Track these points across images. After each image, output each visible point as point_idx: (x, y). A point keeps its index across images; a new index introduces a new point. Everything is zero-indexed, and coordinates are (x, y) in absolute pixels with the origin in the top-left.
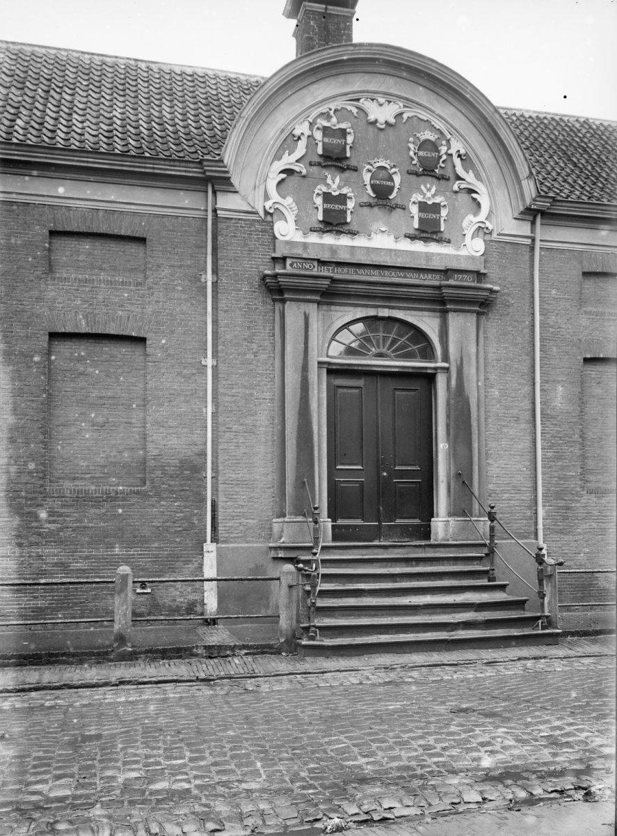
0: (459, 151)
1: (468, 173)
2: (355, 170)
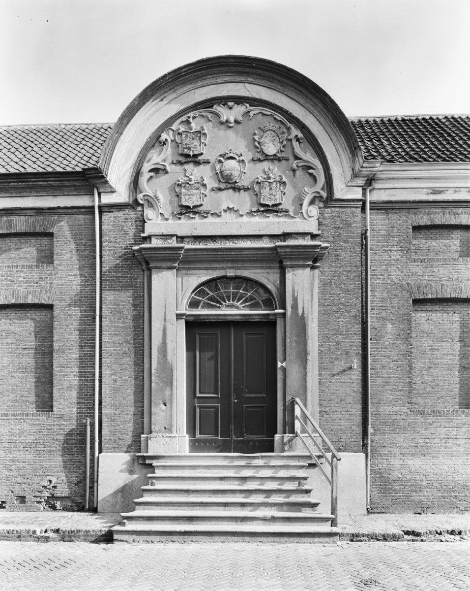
0: (296, 136)
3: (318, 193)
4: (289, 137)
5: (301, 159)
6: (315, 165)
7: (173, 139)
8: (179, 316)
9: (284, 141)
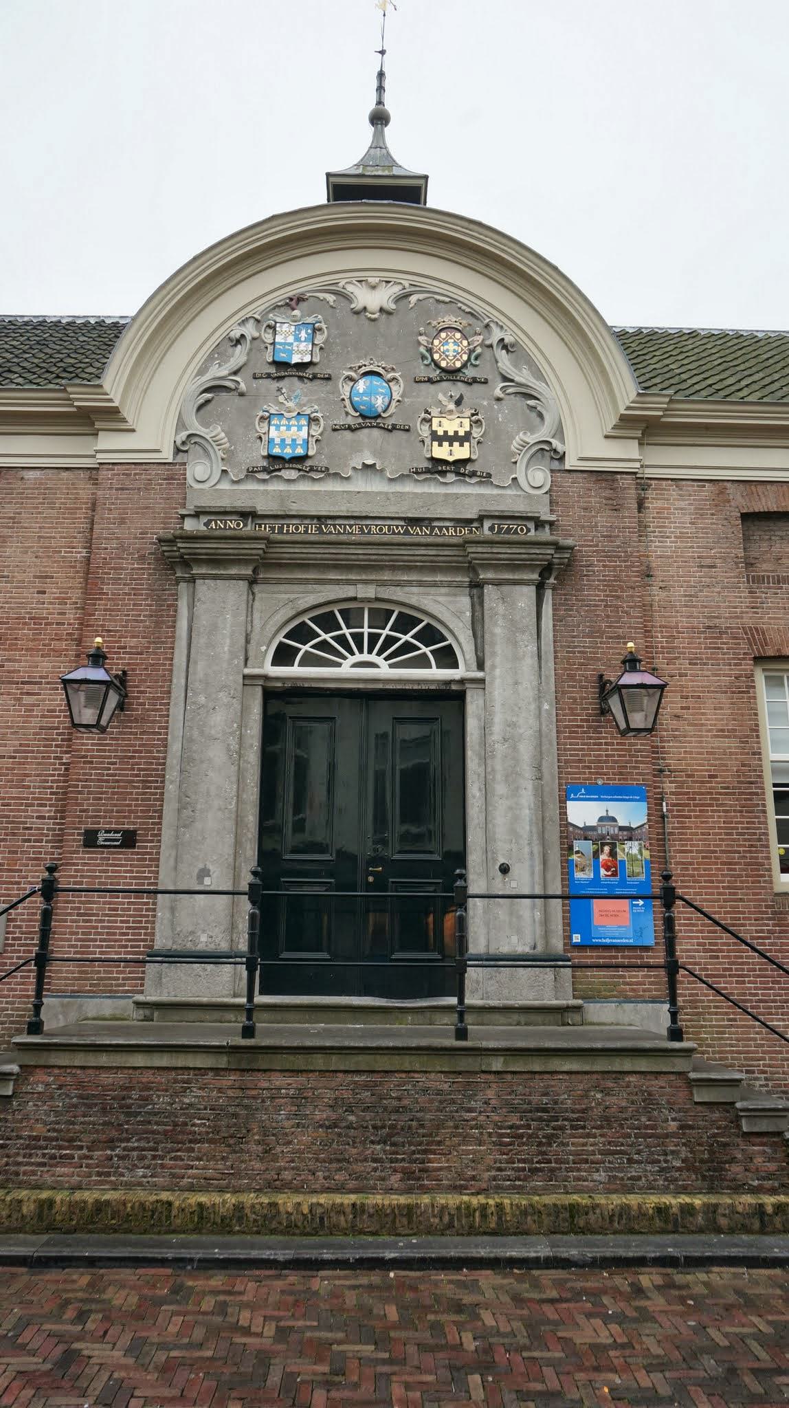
0: (502, 340)
1: (520, 370)
2: (329, 379)
4: (488, 342)
5: (512, 381)
6: (540, 393)
7: (256, 334)
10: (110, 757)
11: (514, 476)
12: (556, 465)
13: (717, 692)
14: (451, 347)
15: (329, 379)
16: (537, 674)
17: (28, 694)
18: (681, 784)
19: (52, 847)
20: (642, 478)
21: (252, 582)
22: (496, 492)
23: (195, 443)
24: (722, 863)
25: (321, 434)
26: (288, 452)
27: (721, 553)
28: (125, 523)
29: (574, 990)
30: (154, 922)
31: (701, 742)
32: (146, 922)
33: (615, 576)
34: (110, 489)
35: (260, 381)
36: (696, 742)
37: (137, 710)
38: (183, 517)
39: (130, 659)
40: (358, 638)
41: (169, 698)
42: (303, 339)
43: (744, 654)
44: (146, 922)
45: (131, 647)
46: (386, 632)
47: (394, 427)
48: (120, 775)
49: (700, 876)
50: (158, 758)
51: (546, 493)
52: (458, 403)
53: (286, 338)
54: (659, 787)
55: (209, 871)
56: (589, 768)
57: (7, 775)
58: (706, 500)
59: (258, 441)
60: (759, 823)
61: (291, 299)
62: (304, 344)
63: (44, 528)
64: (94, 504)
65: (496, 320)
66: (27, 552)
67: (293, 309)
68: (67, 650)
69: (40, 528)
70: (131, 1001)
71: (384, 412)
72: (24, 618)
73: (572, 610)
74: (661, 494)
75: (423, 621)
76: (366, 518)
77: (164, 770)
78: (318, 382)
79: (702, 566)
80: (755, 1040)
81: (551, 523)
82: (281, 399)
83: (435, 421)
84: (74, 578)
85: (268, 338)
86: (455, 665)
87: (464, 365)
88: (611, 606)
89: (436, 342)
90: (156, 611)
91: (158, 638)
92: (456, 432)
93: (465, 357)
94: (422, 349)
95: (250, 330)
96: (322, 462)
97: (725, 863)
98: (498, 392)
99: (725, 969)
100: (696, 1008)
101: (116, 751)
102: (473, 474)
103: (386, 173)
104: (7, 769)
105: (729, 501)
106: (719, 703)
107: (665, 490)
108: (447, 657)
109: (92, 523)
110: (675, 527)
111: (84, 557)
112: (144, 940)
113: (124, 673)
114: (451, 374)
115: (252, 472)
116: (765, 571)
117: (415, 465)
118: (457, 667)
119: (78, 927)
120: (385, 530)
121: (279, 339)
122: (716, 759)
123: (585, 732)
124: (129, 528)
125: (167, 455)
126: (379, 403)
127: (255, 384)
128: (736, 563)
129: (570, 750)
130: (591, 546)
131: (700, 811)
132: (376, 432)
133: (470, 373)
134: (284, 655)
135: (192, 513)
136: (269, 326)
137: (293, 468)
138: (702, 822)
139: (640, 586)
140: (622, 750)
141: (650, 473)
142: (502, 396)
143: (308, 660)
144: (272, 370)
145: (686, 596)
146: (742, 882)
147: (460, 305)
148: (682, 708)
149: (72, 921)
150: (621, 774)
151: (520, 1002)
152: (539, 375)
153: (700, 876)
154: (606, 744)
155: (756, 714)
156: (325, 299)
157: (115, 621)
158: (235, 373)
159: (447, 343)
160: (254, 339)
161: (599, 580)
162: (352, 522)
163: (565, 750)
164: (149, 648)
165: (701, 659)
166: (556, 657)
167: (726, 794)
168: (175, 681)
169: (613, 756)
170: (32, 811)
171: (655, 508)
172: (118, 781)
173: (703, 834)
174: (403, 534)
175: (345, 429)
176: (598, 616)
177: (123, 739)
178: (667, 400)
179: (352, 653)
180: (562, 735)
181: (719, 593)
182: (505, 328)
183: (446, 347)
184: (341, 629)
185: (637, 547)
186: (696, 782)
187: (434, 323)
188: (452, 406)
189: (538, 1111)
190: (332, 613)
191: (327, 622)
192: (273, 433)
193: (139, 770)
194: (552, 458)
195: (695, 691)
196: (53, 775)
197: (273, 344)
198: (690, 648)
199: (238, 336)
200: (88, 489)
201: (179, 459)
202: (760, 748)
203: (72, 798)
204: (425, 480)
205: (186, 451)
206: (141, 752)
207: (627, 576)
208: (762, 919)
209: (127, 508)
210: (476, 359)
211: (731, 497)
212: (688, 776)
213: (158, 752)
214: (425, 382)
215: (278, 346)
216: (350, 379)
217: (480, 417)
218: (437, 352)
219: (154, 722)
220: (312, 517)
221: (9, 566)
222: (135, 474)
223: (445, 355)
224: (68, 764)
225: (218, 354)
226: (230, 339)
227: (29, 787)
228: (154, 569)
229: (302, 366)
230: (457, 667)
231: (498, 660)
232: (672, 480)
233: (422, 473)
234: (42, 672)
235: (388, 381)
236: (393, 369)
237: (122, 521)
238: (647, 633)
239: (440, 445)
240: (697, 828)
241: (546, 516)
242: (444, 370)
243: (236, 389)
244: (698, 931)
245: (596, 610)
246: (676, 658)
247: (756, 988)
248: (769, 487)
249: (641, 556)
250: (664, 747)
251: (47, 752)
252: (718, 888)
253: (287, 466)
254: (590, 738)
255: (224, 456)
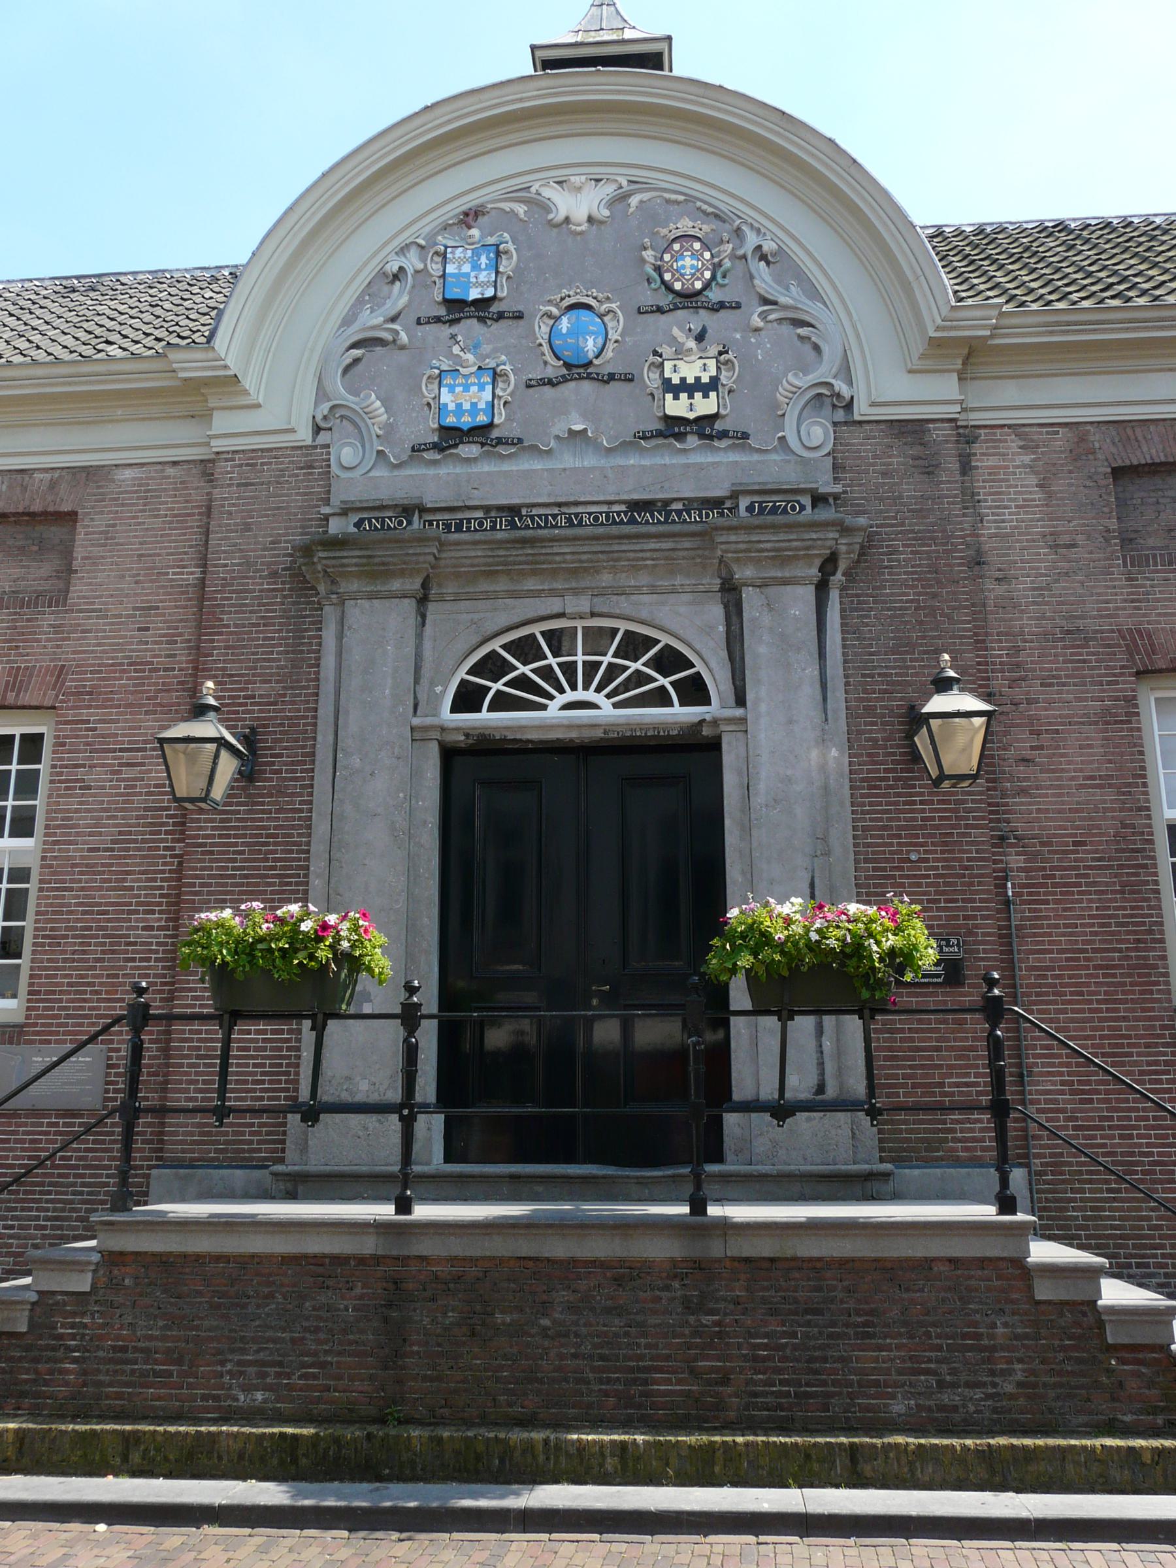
0: (759, 247)
2: (519, 316)
3: (829, 385)
4: (740, 252)
5: (775, 303)
7: (420, 266)
8: (418, 735)
9: (727, 260)
10: (236, 844)
11: (780, 435)
12: (840, 415)
13: (1081, 723)
14: (688, 262)
15: (519, 316)
16: (820, 707)
17: (128, 765)
18: (1032, 856)
19: (164, 968)
20: (966, 427)
21: (423, 600)
22: (756, 457)
23: (342, 417)
24: (1096, 967)
25: (511, 394)
26: (466, 421)
27: (1084, 525)
28: (249, 530)
29: (882, 1150)
30: (298, 1065)
31: (1061, 795)
32: (288, 1065)
33: (928, 566)
34: (230, 485)
35: (427, 327)
36: (1054, 795)
37: (271, 780)
38: (326, 518)
39: (260, 711)
40: (569, 669)
41: (313, 762)
42: (483, 266)
43: (1122, 667)
44: (288, 1065)
45: (261, 696)
46: (607, 659)
47: (612, 377)
48: (248, 868)
49: (1062, 985)
50: (299, 844)
51: (828, 454)
52: (700, 338)
53: (459, 268)
54: (1001, 861)
55: (369, 994)
56: (899, 836)
57: (103, 873)
58: (1061, 452)
59: (426, 408)
60: (1150, 908)
61: (466, 214)
62: (485, 273)
63: (145, 543)
64: (209, 508)
65: (750, 220)
66: (124, 576)
67: (469, 227)
68: (179, 704)
69: (141, 543)
70: (266, 1172)
71: (597, 357)
72: (122, 664)
73: (869, 617)
74: (994, 447)
75: (658, 641)
76: (577, 504)
77: (307, 859)
78: (503, 323)
79: (1057, 546)
80: (1149, 1218)
81: (836, 497)
82: (456, 350)
83: (668, 365)
84: (186, 607)
85: (435, 268)
86: (707, 701)
87: (707, 286)
88: (924, 608)
89: (667, 257)
90: (293, 645)
91: (298, 681)
92: (698, 379)
93: (708, 275)
94: (649, 270)
95: (412, 262)
96: (514, 431)
97: (1100, 967)
98: (756, 321)
99: (1102, 1119)
100: (1061, 1174)
101: (244, 836)
102: (724, 435)
103: (614, 37)
104: (103, 865)
105: (1094, 453)
106: (1087, 738)
107: (1000, 441)
108: (694, 692)
109: (207, 533)
110: (1016, 493)
111: (197, 579)
112: (287, 1090)
113: (253, 729)
114: (689, 299)
115: (419, 451)
116: (1148, 549)
117: (642, 428)
118: (709, 704)
119: (197, 1074)
120: (602, 518)
121: (450, 269)
122: (1081, 819)
123: (891, 787)
124: (256, 536)
125: (304, 435)
126: (590, 346)
127: (420, 331)
128: (1107, 540)
129: (868, 812)
130: (893, 525)
131: (1062, 893)
132: (586, 386)
133: (714, 295)
134: (467, 699)
135: (338, 511)
136: (436, 253)
137: (473, 442)
138: (1065, 909)
139: (965, 578)
140: (945, 811)
141: (976, 418)
142: (761, 324)
143: (502, 703)
144: (442, 311)
145: (1034, 589)
146: (1124, 993)
147: (699, 204)
148: (1032, 748)
149: (190, 1065)
150: (945, 844)
151: (802, 1168)
152: (814, 294)
153: (1062, 985)
154: (922, 802)
155: (1142, 753)
156: (512, 211)
157: (241, 661)
158: (393, 319)
159: (682, 257)
160: (417, 272)
161: (905, 573)
162: (556, 511)
163: (863, 812)
164: (284, 695)
165: (1059, 677)
166: (847, 684)
167: (1100, 868)
168: (319, 738)
169: (933, 819)
170: (137, 920)
171: (987, 467)
172: (246, 877)
173: (1066, 926)
174: (629, 523)
175: (544, 384)
176: (906, 623)
177: (254, 820)
178: (995, 313)
179: (562, 691)
180: (858, 792)
181: (1082, 583)
182: (763, 230)
183: (680, 263)
184: (546, 658)
185: (961, 523)
186: (1056, 852)
187: (664, 231)
188: (691, 344)
189: (808, 1314)
190: (533, 636)
191: (526, 649)
192: (446, 397)
193: (275, 860)
194: (834, 406)
195: (1050, 724)
196: (163, 872)
197: (444, 276)
198: (1042, 662)
199: (395, 269)
200: (202, 488)
201: (323, 438)
202: (1148, 801)
203: (187, 902)
204: (657, 447)
205: (330, 429)
206: (275, 836)
207: (945, 565)
208: (1156, 1045)
209: (252, 510)
210: (724, 277)
211: (1097, 445)
212: (1043, 844)
213: (299, 835)
214: (652, 312)
215: (449, 279)
216: (549, 315)
217: (730, 356)
218: (668, 271)
219: (293, 795)
220: (500, 508)
221: (101, 597)
222: (262, 464)
223: (678, 274)
224: (180, 856)
225: (370, 295)
226: (385, 275)
227: (131, 888)
228: (290, 589)
229: (483, 304)
230: (709, 704)
231: (763, 692)
232: (1009, 426)
233: (652, 437)
234: (146, 734)
235: (601, 316)
236: (608, 298)
237: (247, 528)
238: (980, 644)
239: (676, 398)
240: (1057, 917)
241: (826, 486)
242: (678, 294)
243: (394, 341)
244: (1061, 1065)
245: (902, 615)
246: (1024, 679)
247: (1148, 1145)
248: (1152, 428)
249: (967, 536)
250: (1007, 804)
251: (154, 841)
252: (1090, 1002)
253: (465, 439)
254: (899, 795)
255: (380, 432)
